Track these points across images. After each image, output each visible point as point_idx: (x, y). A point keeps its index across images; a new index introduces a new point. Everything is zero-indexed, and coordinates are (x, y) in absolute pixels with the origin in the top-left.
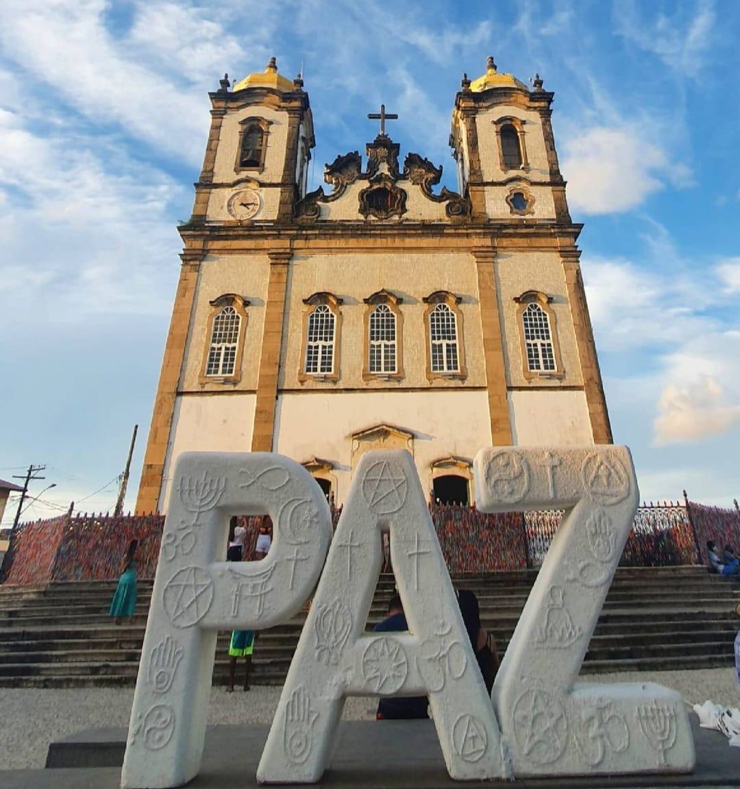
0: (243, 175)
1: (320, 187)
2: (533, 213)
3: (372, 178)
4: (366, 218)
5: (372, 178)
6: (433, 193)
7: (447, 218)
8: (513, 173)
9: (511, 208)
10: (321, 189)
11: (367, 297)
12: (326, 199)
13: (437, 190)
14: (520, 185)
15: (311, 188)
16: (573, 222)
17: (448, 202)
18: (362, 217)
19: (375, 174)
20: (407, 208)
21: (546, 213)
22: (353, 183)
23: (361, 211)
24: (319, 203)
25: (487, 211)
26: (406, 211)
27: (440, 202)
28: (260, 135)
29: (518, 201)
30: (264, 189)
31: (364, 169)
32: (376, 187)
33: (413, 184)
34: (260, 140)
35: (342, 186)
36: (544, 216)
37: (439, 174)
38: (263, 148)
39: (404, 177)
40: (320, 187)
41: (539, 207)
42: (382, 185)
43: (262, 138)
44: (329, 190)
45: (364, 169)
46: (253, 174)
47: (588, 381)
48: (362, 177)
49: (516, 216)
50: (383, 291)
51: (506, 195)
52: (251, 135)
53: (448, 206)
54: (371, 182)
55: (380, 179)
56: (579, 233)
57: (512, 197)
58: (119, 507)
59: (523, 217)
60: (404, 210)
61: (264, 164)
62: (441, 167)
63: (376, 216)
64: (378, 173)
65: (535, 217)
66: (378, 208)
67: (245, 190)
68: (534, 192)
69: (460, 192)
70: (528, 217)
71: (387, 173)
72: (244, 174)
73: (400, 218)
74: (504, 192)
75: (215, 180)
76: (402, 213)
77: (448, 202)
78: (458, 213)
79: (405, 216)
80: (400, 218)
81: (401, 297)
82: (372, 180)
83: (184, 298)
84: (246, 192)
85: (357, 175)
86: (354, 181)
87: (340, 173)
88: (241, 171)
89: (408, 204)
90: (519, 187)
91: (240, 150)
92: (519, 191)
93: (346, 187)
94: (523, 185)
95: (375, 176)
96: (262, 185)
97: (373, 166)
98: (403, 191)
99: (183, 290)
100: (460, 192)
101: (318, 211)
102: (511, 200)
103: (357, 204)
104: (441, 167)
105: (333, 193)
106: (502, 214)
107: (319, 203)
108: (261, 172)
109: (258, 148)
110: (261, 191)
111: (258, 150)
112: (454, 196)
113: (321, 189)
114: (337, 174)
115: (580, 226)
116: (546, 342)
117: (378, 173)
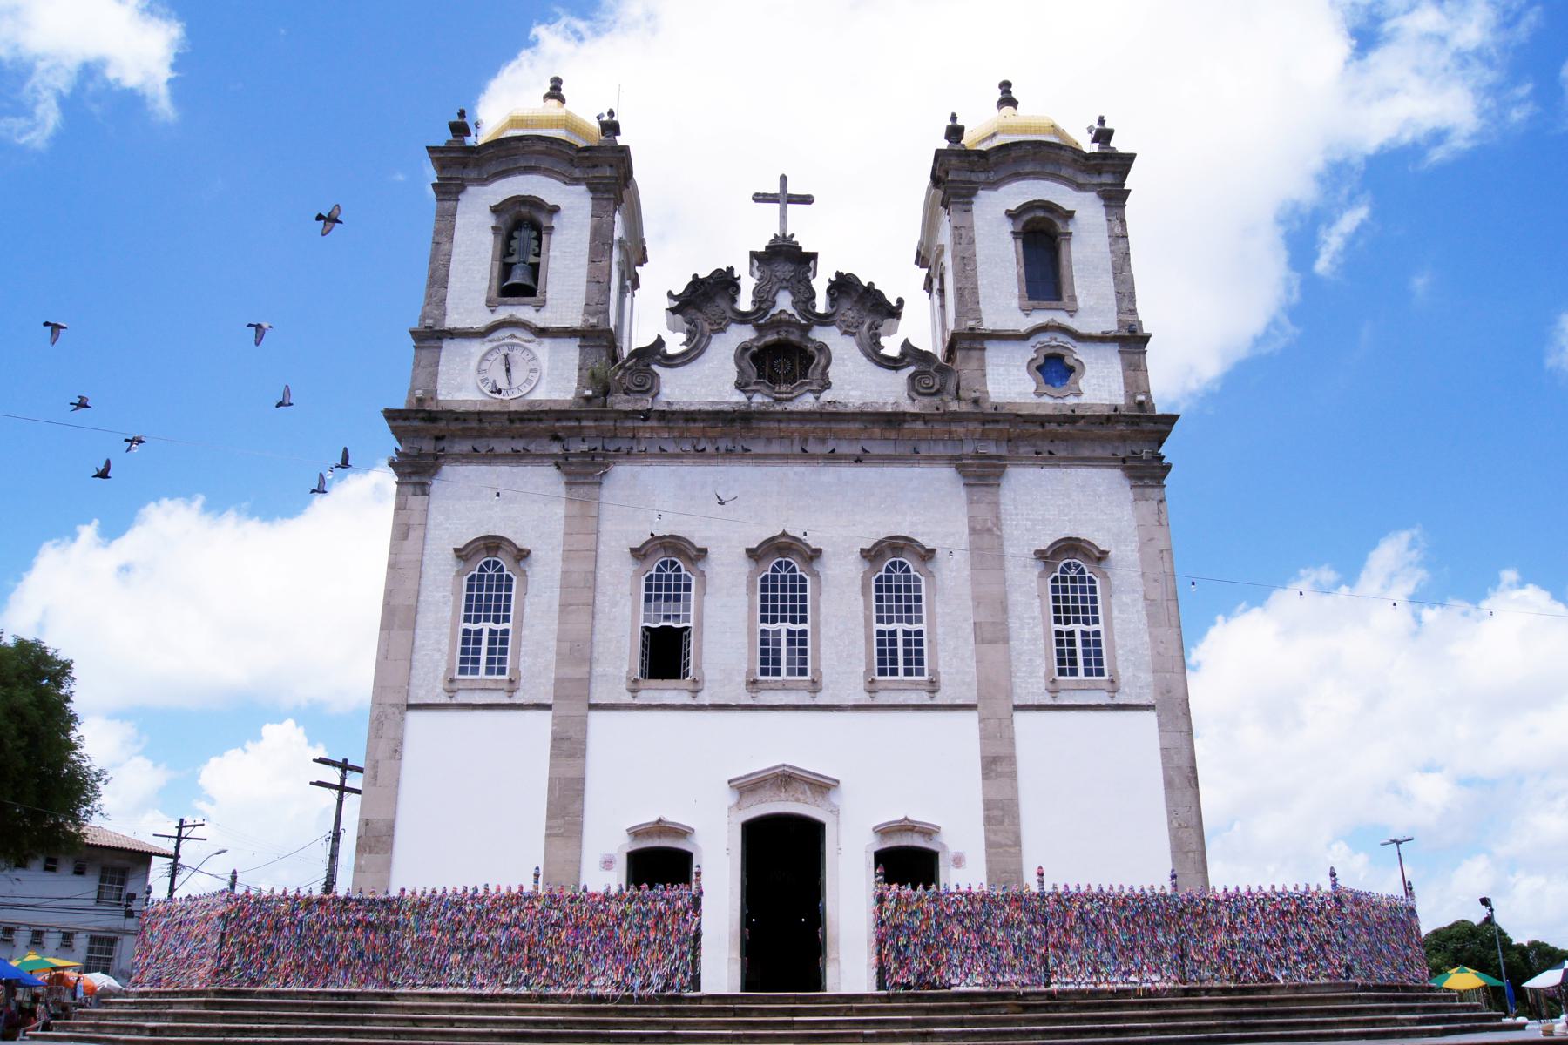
0: (503, 313)
1: (659, 337)
2: (1079, 394)
3: (762, 322)
4: (749, 398)
5: (762, 322)
6: (882, 352)
7: (909, 402)
8: (1040, 318)
9: (1037, 383)
10: (659, 342)
11: (755, 546)
12: (671, 361)
13: (891, 347)
14: (1055, 339)
15: (640, 337)
16: (1158, 411)
17: (912, 369)
18: (739, 398)
19: (766, 312)
20: (831, 380)
21: (1105, 396)
22: (723, 330)
23: (741, 386)
24: (655, 367)
25: (990, 388)
26: (826, 385)
27: (896, 369)
28: (534, 234)
29: (1054, 368)
30: (547, 342)
31: (745, 303)
32: (770, 338)
33: (845, 333)
34: (536, 243)
35: (702, 335)
36: (1101, 400)
37: (894, 312)
38: (542, 259)
39: (824, 320)
40: (659, 337)
41: (1093, 381)
42: (783, 335)
43: (539, 239)
44: (675, 343)
45: (745, 303)
46: (525, 312)
47: (1162, 694)
48: (743, 318)
49: (1046, 400)
50: (784, 534)
51: (1030, 358)
52: (516, 234)
53: (912, 377)
54: (759, 328)
55: (779, 323)
56: (1167, 433)
57: (1041, 361)
58: (330, 884)
59: (1059, 401)
60: (826, 385)
61: (545, 292)
62: (901, 301)
63: (769, 396)
64: (775, 311)
65: (1084, 400)
66: (774, 380)
67: (509, 341)
68: (1081, 353)
69: (939, 352)
70: (1071, 401)
71: (791, 311)
72: (503, 313)
73: (817, 398)
74: (1025, 353)
75: (452, 322)
76: (820, 392)
77: (912, 369)
78: (933, 391)
79: (827, 396)
80: (817, 398)
81: (818, 547)
82: (762, 325)
83: (405, 542)
84: (513, 345)
85: (729, 314)
86: (727, 325)
87: (701, 311)
88: (501, 304)
89: (833, 373)
90: (1054, 343)
91: (497, 264)
92: (1052, 351)
93: (710, 337)
94: (1062, 339)
95: (769, 317)
96: (542, 332)
97: (763, 298)
98: (823, 349)
99: (402, 532)
100: (939, 352)
101: (649, 386)
102: (1039, 368)
103: (732, 373)
104: (901, 301)
105: (684, 348)
106: (1020, 394)
107: (655, 367)
108: (540, 306)
109: (532, 259)
110: (540, 344)
111: (531, 264)
112: (924, 357)
113: (659, 342)
114: (692, 312)
115: (1171, 420)
116: (1091, 628)
117: (775, 311)
